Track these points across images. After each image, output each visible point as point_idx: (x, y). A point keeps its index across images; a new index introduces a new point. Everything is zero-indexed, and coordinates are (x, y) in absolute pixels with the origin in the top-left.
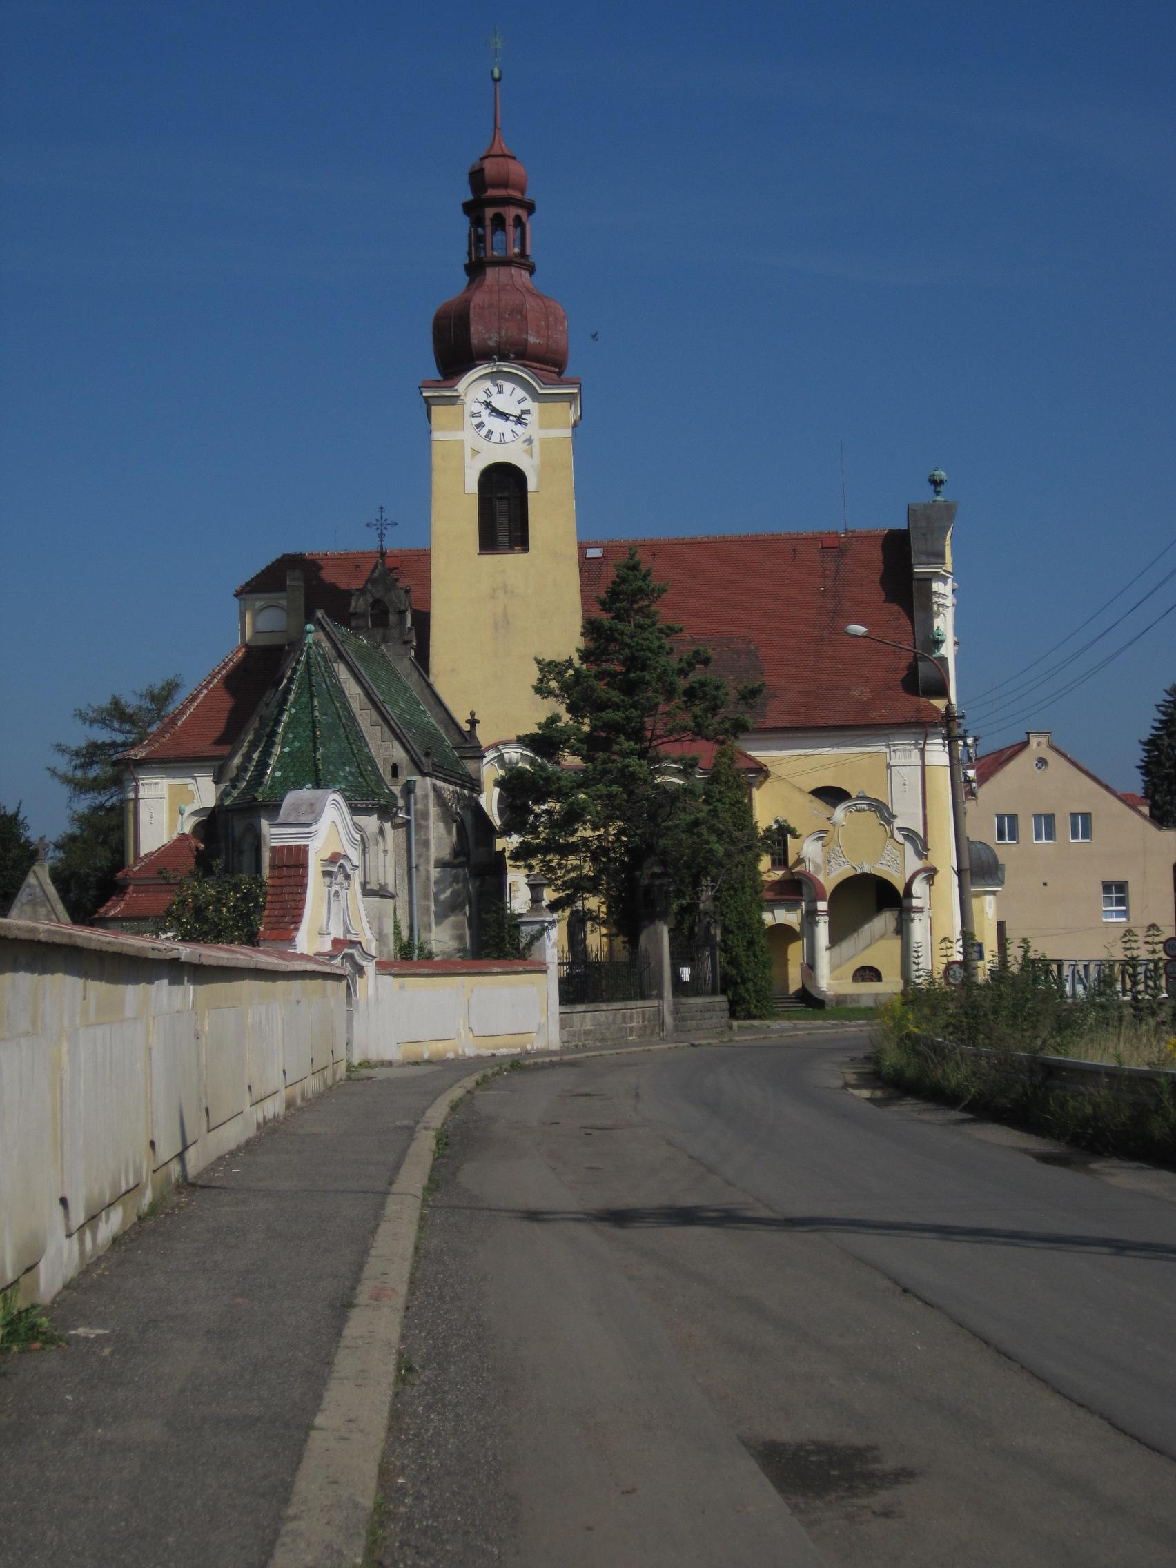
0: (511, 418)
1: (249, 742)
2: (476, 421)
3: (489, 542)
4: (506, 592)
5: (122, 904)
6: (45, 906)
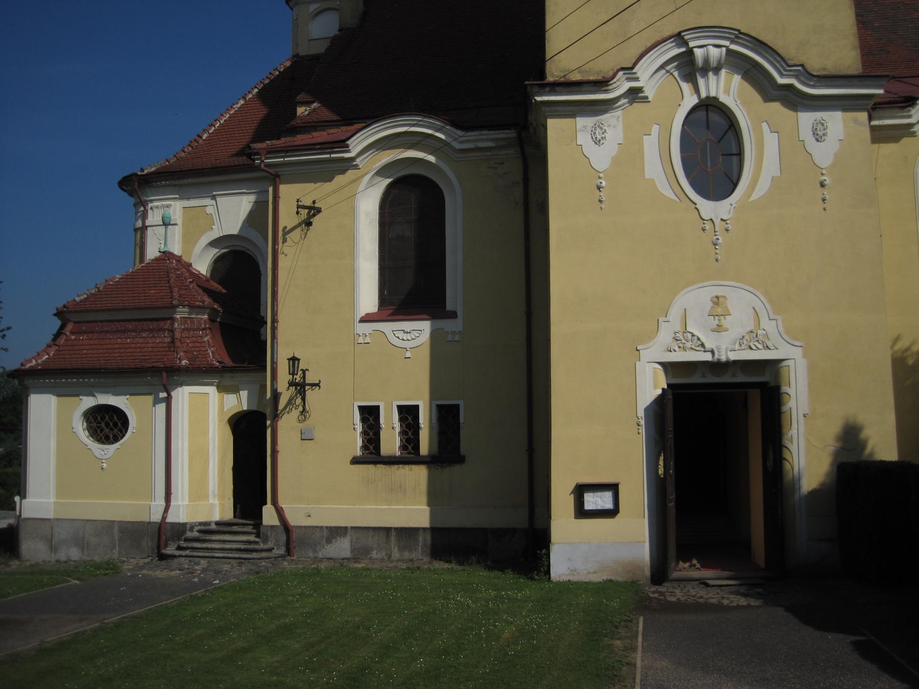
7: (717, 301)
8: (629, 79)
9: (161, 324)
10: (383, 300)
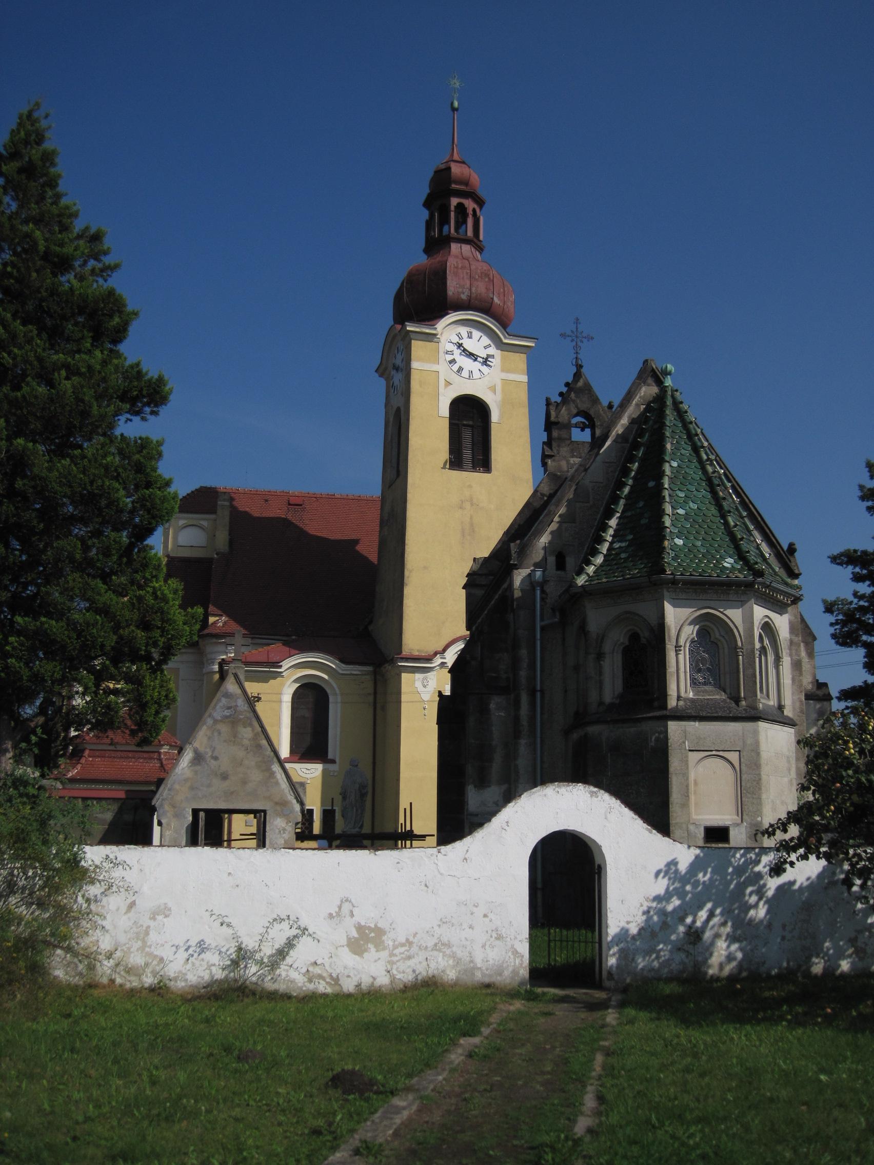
0: (479, 359)
1: (560, 516)
2: (449, 358)
3: (456, 462)
4: (472, 505)
5: (79, 767)
6: (251, 725)
8: (441, 658)
9: (152, 755)
10: (292, 751)
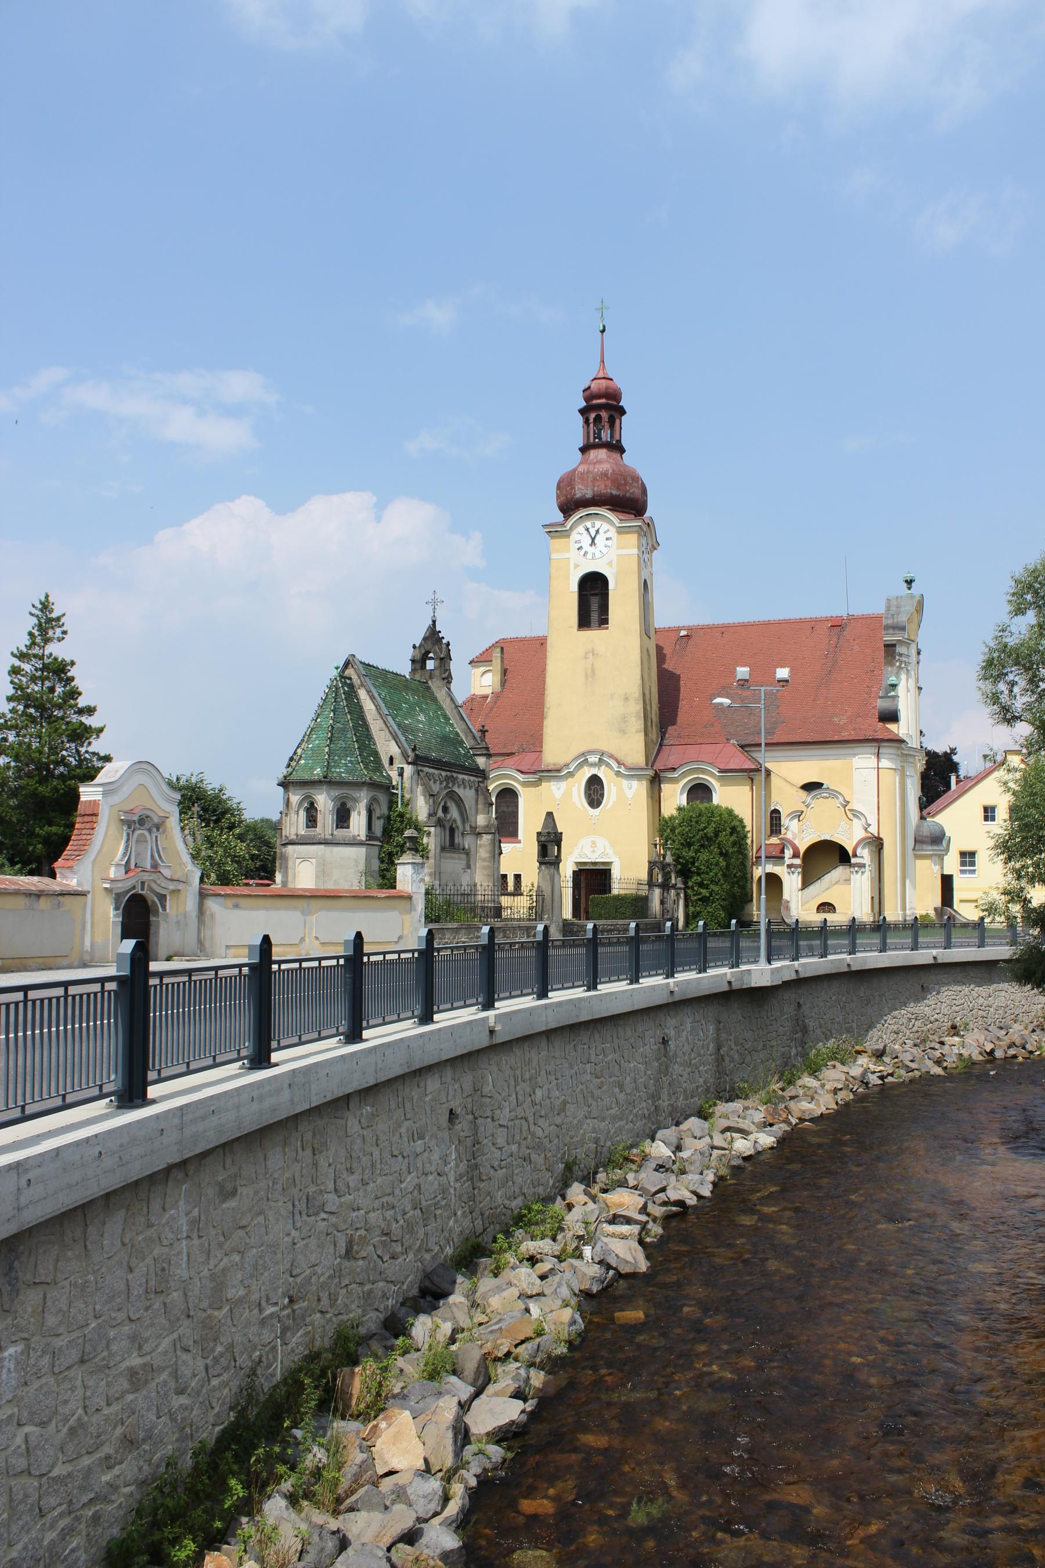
2: (578, 545)
3: (584, 622)
4: (593, 655)
7: (593, 842)
